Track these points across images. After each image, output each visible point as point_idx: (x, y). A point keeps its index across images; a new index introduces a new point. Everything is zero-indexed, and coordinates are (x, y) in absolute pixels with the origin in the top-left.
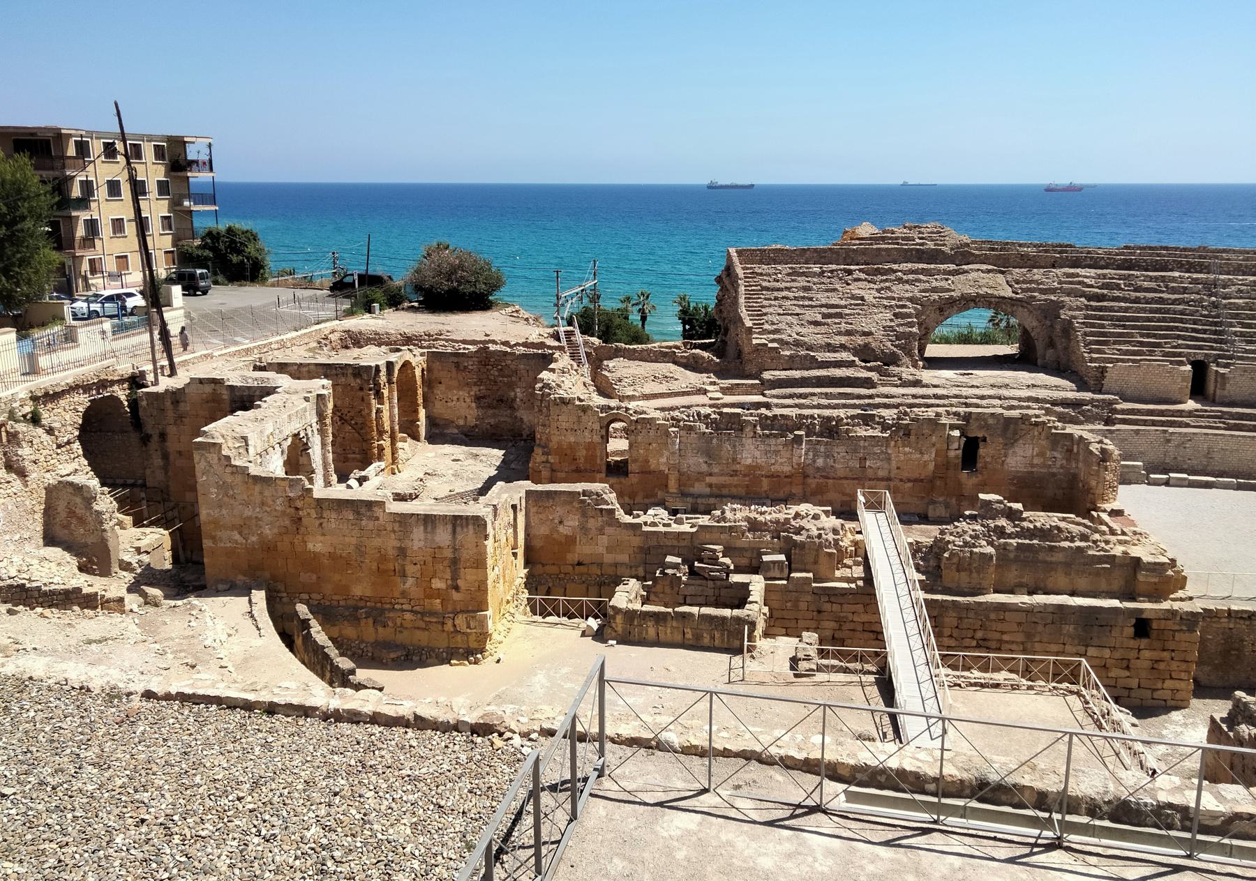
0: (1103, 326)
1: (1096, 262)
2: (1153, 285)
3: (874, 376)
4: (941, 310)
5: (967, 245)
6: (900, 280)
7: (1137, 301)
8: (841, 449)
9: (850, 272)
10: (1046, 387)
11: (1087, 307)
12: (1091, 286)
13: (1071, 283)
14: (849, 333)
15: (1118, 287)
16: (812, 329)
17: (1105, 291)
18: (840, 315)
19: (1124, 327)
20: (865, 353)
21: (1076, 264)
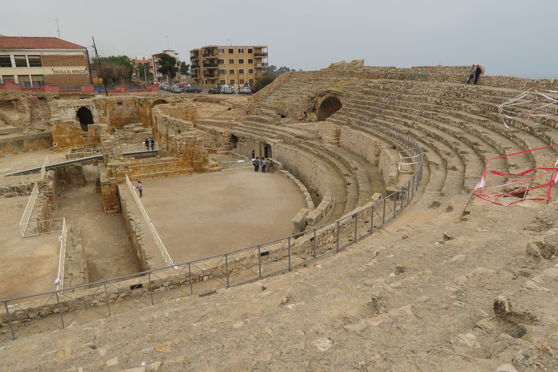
12: (370, 87)
18: (286, 97)
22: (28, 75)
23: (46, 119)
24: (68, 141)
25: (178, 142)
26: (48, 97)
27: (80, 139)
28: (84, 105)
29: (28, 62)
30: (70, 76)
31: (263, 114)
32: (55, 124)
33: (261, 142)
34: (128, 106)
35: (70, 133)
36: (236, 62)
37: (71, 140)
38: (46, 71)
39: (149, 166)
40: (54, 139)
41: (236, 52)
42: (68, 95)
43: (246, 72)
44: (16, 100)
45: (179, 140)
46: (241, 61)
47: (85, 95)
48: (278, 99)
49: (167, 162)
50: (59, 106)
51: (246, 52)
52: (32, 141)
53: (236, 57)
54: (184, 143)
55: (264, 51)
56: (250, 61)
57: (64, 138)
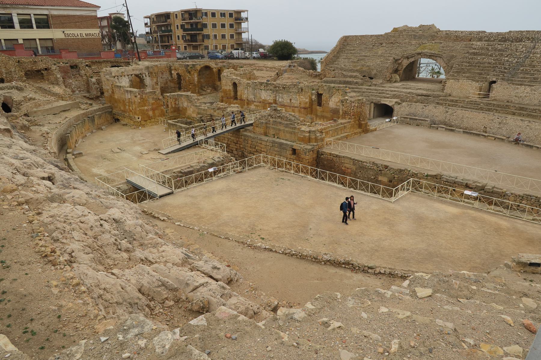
1: (489, 39)
8: (285, 95)
9: (382, 44)
10: (424, 89)
12: (475, 49)
14: (363, 66)
21: (480, 40)
22: (35, 39)
23: (80, 91)
24: (151, 113)
25: (353, 104)
26: (80, 65)
27: (162, 111)
29: (34, 22)
30: (83, 41)
31: (345, 76)
33: (372, 102)
34: (162, 73)
35: (153, 104)
36: (219, 26)
37: (154, 113)
38: (55, 34)
41: (218, 15)
42: (99, 62)
43: (227, 37)
44: (46, 69)
45: (353, 102)
46: (223, 26)
47: (116, 62)
49: (345, 125)
50: (113, 75)
51: (227, 15)
57: (147, 110)
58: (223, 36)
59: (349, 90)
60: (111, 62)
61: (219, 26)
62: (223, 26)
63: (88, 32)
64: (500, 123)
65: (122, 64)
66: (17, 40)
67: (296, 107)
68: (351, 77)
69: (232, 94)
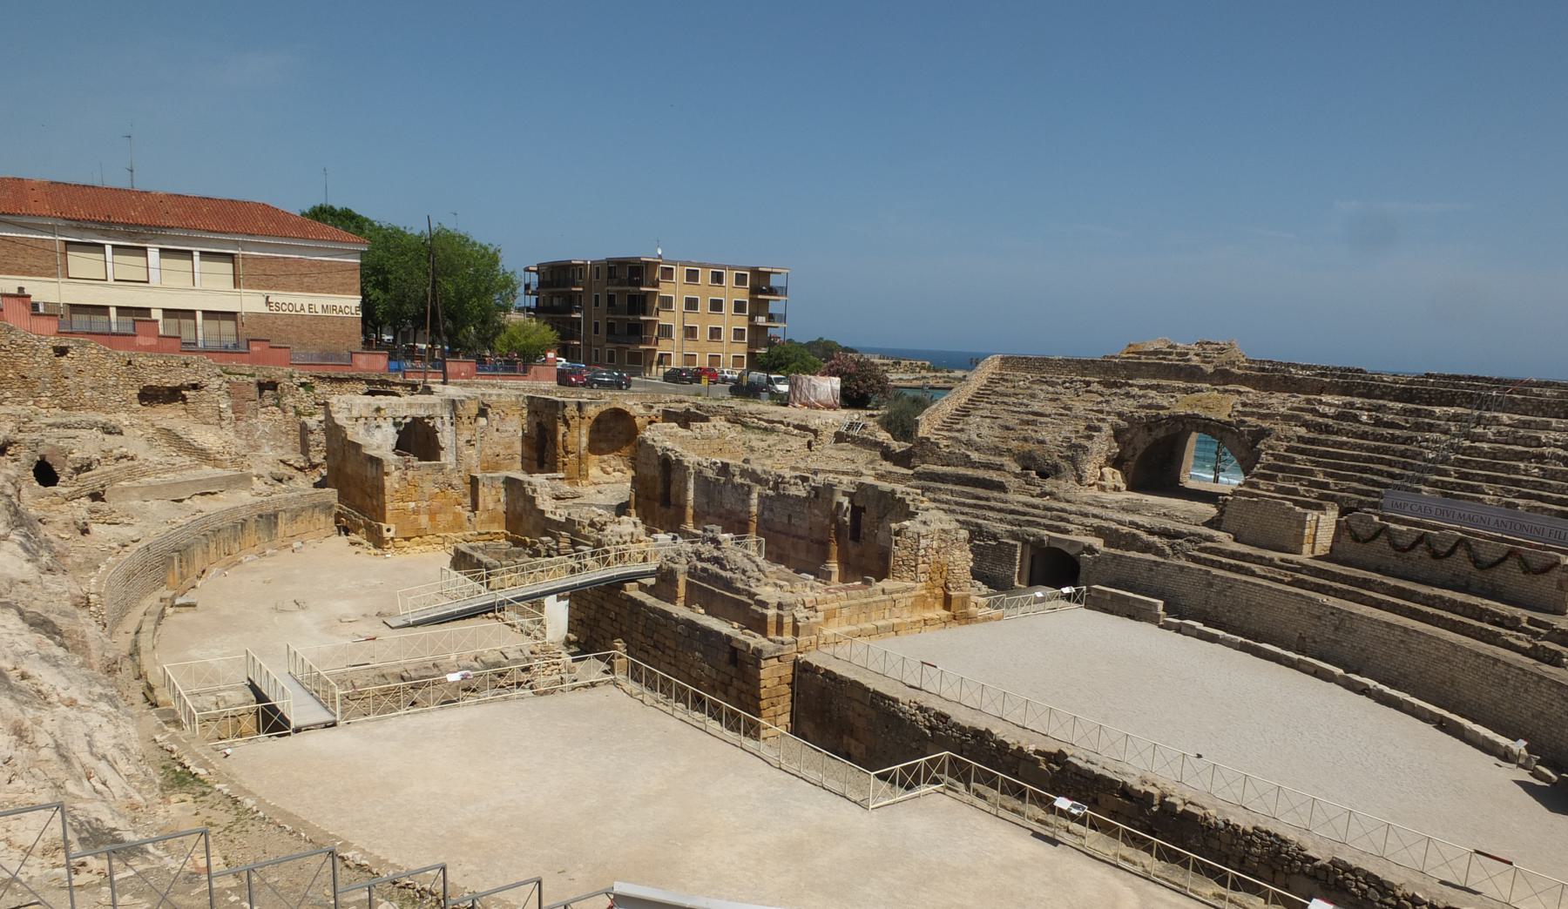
0: (1293, 460)
2: (1399, 420)
3: (1012, 482)
4: (1150, 430)
5: (1233, 363)
6: (1128, 395)
7: (1364, 436)
9: (1088, 384)
11: (1300, 439)
12: (1325, 415)
13: (1302, 410)
14: (1025, 440)
15: (1356, 419)
16: (997, 432)
17: (1330, 422)
19: (1318, 464)
20: (1027, 461)
26: (285, 383)
27: (457, 516)
28: (422, 413)
32: (397, 469)
35: (433, 497)
36: (704, 306)
39: (860, 605)
40: (388, 515)
41: (705, 276)
44: (195, 387)
46: (716, 306)
48: (1008, 428)
49: (895, 596)
50: (355, 413)
52: (295, 516)
53: (704, 291)
54: (935, 544)
55: (774, 281)
56: (739, 307)
58: (715, 333)
59: (927, 504)
60: (369, 382)
61: (704, 306)
62: (716, 306)
63: (331, 302)
64: (1337, 629)
65: (398, 389)
66: (149, 309)
67: (800, 538)
68: (987, 466)
69: (659, 489)
